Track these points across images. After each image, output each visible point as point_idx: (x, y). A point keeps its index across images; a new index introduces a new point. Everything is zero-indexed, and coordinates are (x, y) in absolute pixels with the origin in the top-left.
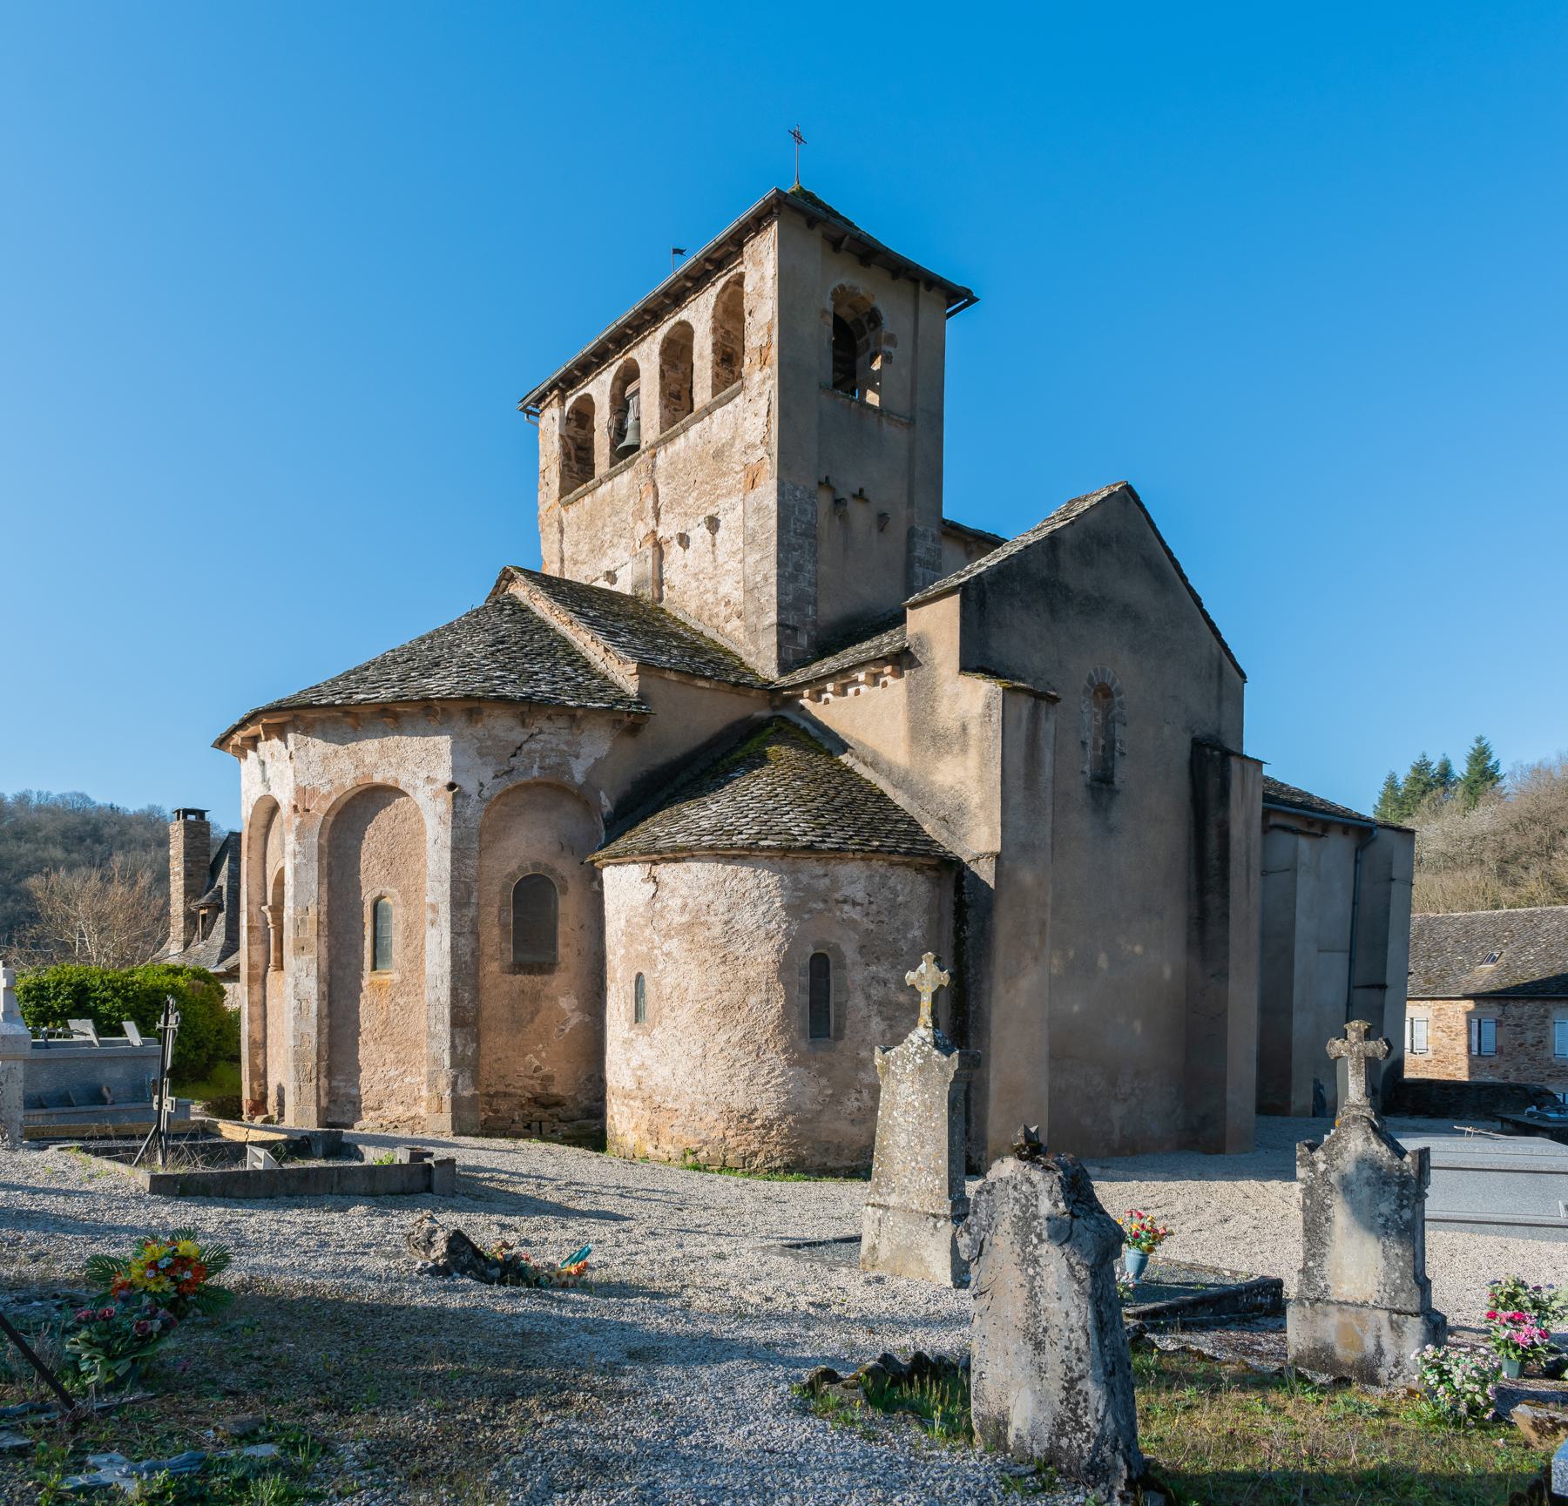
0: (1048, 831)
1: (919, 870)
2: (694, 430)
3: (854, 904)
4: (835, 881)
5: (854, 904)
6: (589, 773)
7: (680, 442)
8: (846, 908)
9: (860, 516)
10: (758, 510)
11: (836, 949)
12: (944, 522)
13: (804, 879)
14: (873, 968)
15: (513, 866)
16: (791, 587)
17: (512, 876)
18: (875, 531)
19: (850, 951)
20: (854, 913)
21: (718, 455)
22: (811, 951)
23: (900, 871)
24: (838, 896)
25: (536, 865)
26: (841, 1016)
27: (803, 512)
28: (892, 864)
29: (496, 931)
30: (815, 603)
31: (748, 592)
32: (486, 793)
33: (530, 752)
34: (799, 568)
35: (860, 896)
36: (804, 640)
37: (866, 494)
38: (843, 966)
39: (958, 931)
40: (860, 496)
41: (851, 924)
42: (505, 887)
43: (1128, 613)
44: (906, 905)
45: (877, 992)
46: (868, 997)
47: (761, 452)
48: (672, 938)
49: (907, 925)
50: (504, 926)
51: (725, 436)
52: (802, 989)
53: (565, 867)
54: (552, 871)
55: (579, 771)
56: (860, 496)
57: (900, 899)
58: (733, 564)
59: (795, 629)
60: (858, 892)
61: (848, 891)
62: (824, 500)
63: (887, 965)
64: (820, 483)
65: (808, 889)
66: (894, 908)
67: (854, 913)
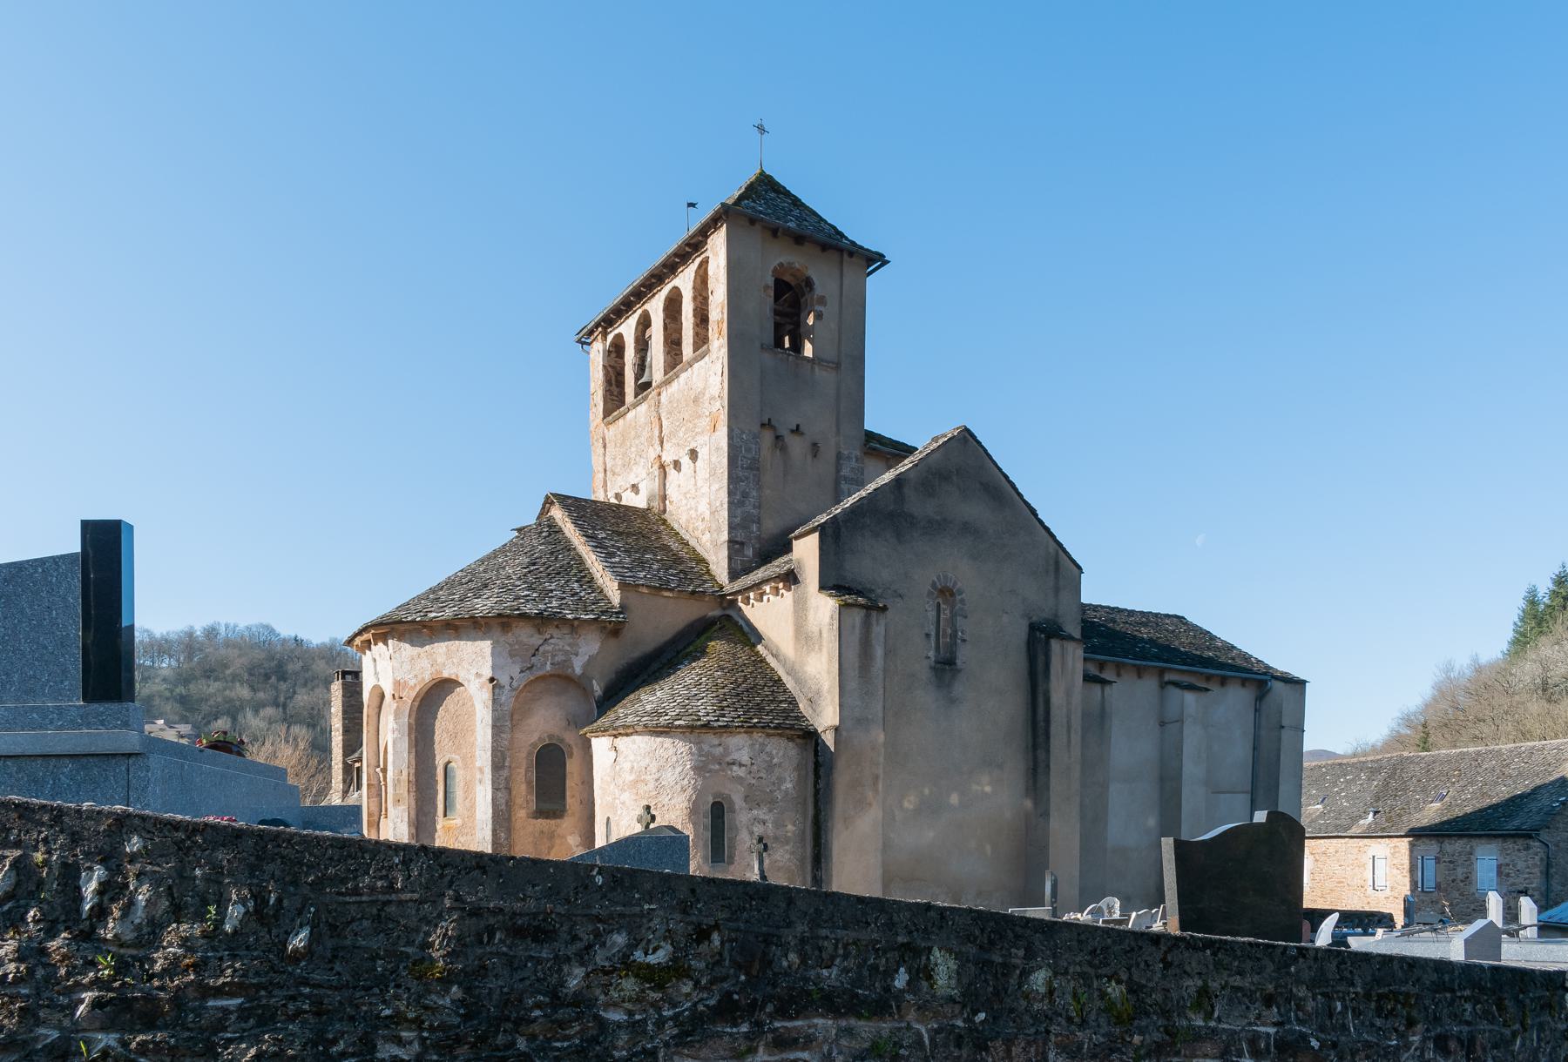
0: (880, 707)
1: (790, 739)
2: (683, 376)
3: (741, 765)
4: (726, 749)
5: (741, 765)
6: (586, 666)
7: (675, 385)
8: (735, 768)
9: (797, 446)
11: (729, 798)
12: (870, 436)
13: (706, 748)
14: (755, 812)
15: (535, 738)
16: (739, 511)
17: (534, 745)
18: (809, 458)
19: (738, 800)
20: (741, 772)
21: (696, 400)
22: (711, 800)
23: (774, 740)
24: (728, 759)
25: (551, 736)
26: (732, 847)
27: (749, 450)
28: (768, 735)
29: (524, 787)
30: (759, 522)
31: (712, 513)
32: (515, 684)
33: (545, 652)
34: (745, 495)
35: (745, 759)
36: (749, 552)
37: (802, 428)
38: (733, 811)
39: (816, 783)
40: (797, 431)
41: (740, 780)
42: (530, 754)
43: (967, 529)
44: (780, 765)
45: (758, 830)
46: (752, 833)
48: (623, 790)
49: (781, 780)
50: (529, 783)
51: (700, 385)
52: (705, 828)
53: (570, 738)
54: (562, 741)
55: (578, 666)
56: (797, 431)
57: (775, 761)
58: (705, 489)
59: (742, 544)
60: (744, 757)
61: (735, 756)
62: (767, 437)
63: (765, 810)
64: (763, 425)
65: (708, 754)
66: (770, 767)
67: (741, 772)
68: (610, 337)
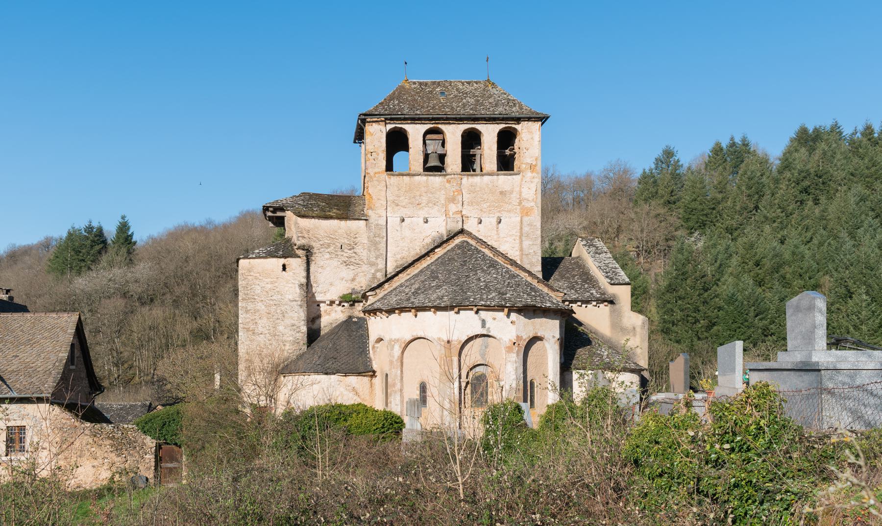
10: (530, 225)
47: (533, 204)
68: (390, 127)
